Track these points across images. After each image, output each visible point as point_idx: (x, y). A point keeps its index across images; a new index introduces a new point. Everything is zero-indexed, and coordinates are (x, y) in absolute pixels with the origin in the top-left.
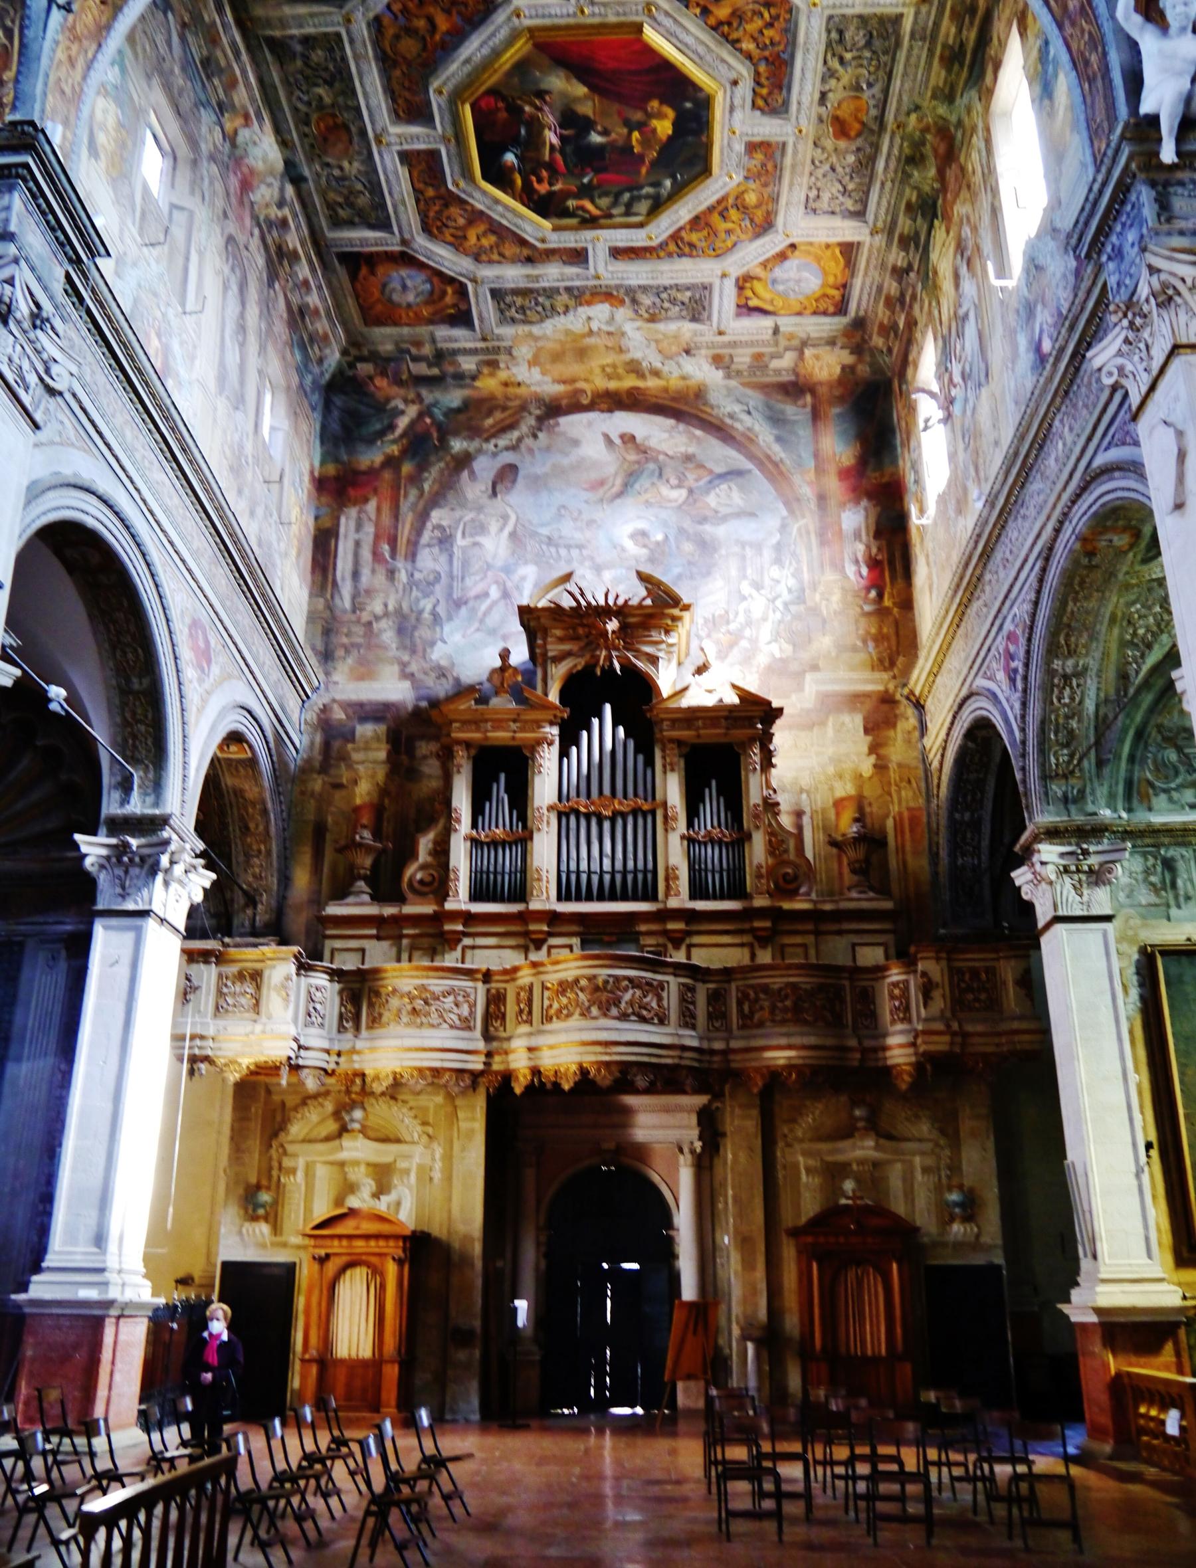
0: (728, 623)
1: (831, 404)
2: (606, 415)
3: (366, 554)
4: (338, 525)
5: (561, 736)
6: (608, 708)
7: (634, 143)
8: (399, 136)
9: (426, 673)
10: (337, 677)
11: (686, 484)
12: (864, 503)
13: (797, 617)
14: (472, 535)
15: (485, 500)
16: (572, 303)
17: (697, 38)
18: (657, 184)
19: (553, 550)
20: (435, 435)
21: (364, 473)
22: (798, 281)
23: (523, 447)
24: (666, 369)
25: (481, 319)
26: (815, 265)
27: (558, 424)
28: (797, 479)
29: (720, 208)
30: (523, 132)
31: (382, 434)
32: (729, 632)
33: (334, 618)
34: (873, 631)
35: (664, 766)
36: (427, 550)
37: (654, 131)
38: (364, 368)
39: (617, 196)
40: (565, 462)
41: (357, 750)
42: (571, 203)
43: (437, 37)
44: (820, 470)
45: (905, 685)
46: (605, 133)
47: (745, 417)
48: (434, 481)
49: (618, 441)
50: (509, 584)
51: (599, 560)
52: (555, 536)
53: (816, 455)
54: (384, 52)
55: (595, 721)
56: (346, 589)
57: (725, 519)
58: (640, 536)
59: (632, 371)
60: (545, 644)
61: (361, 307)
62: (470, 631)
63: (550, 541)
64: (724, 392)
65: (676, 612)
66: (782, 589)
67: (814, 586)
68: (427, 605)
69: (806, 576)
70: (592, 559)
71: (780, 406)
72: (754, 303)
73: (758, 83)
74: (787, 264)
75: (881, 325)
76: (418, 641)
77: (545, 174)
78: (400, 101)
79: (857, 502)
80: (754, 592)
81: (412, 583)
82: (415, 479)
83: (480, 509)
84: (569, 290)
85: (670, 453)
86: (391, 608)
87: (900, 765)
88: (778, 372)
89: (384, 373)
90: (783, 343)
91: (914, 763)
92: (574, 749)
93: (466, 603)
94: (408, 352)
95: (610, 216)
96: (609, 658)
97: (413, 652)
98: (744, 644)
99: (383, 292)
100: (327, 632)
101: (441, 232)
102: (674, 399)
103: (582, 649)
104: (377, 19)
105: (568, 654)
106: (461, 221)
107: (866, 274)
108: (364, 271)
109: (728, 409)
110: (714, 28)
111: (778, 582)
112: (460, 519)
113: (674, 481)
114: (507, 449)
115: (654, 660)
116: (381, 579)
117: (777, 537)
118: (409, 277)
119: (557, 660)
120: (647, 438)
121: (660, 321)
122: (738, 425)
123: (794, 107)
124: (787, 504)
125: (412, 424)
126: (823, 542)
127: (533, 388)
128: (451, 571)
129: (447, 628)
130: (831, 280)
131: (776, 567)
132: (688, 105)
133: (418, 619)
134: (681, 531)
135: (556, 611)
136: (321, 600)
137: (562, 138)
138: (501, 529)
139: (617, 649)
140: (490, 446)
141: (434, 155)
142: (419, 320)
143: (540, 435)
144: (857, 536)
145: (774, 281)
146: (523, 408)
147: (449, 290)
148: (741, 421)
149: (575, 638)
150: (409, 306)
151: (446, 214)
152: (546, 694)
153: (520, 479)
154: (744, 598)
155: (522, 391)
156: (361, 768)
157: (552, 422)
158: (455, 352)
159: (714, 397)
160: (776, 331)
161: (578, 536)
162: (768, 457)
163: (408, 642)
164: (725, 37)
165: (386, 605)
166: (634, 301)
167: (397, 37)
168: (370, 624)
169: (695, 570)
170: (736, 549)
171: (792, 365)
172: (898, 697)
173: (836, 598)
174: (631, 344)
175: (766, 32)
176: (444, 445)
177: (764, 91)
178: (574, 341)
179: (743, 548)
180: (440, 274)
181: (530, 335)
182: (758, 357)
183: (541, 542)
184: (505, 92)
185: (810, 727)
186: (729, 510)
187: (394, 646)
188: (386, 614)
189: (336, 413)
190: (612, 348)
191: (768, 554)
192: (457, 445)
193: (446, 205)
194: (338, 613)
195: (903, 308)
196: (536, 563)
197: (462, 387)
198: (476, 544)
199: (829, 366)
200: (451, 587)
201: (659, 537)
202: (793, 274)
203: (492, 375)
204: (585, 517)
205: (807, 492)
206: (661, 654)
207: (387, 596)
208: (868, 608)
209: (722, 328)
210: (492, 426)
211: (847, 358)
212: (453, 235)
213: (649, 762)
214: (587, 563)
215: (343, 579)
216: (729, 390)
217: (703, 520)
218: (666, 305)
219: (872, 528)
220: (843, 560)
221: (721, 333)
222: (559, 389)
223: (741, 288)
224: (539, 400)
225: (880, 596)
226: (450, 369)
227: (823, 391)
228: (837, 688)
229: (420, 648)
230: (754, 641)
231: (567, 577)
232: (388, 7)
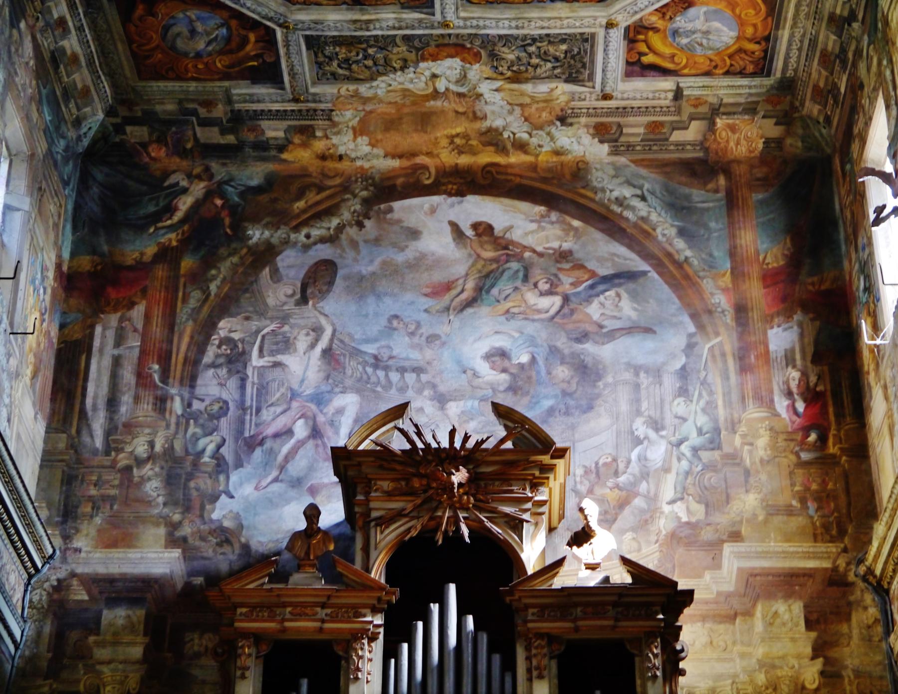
0: (616, 474)
1: (751, 188)
2: (454, 199)
3: (128, 376)
4: (91, 336)
5: (386, 625)
6: (452, 589)
9: (203, 539)
10: (78, 543)
11: (559, 289)
12: (798, 316)
13: (710, 467)
14: (272, 353)
15: (290, 306)
16: (412, 56)
19: (381, 373)
20: (227, 221)
21: (130, 268)
22: (707, 32)
23: (343, 237)
24: (534, 141)
25: (293, 75)
26: (728, 12)
27: (391, 210)
28: (707, 285)
31: (156, 217)
32: (617, 486)
33: (79, 461)
34: (814, 487)
35: (529, 671)
36: (211, 372)
38: (136, 133)
40: (400, 258)
41: (102, 644)
44: (737, 274)
45: (861, 561)
47: (636, 203)
48: (224, 280)
49: (469, 233)
50: (321, 419)
51: (442, 388)
52: (385, 354)
53: (733, 254)
55: (435, 608)
56: (98, 424)
57: (611, 335)
58: (498, 356)
59: (490, 144)
60: (368, 501)
61: (134, 55)
62: (264, 483)
63: (377, 362)
64: (612, 172)
65: (546, 459)
66: (689, 429)
67: (733, 426)
68: (208, 444)
69: (721, 413)
70: (434, 386)
71: (687, 190)
72: (649, 59)
75: (816, 87)
76: (195, 494)
79: (789, 317)
80: (652, 434)
81: (189, 416)
82: (199, 278)
83: (284, 319)
84: (407, 39)
85: (539, 249)
86: (158, 448)
87: (858, 673)
88: (681, 146)
89: (161, 141)
90: (687, 110)
91: (877, 671)
92: (405, 646)
93: (261, 443)
94: (194, 113)
96: (455, 521)
97: (187, 509)
98: (638, 502)
99: (164, 37)
100: (69, 480)
102: (544, 180)
103: (416, 508)
105: (398, 515)
107: (794, 25)
108: (140, 10)
109: (616, 194)
111: (685, 420)
112: (258, 332)
113: (544, 286)
114: (322, 240)
115: (516, 525)
116: (146, 409)
117: (683, 360)
118: (199, 18)
119: (384, 522)
120: (510, 228)
121: (527, 80)
122: (628, 214)
124: (694, 316)
125: (197, 206)
126: (744, 368)
127: (359, 163)
128: (243, 402)
129: (234, 477)
130: (750, 31)
131: (680, 400)
133: (196, 464)
134: (553, 351)
135: (384, 454)
136: (65, 435)
138: (312, 346)
139: (466, 509)
140: (302, 237)
142: (211, 73)
143: (367, 223)
144: (789, 359)
145: (675, 33)
146: (346, 188)
147: (252, 37)
148: (633, 209)
149: (410, 493)
150: (198, 55)
152: (368, 570)
153: (339, 281)
154: (638, 441)
155: (344, 165)
156: (105, 669)
157: (382, 206)
158: (258, 115)
159: (598, 178)
160: (678, 94)
161: (415, 355)
162: (669, 255)
163: (180, 495)
165: (152, 444)
166: (494, 56)
168: (128, 469)
169: (572, 403)
170: (628, 376)
171: (700, 138)
172: (851, 577)
173: (763, 441)
174: (488, 109)
176: (239, 235)
178: (414, 103)
179: (637, 374)
181: (356, 95)
182: (654, 127)
183: (365, 364)
185: (731, 618)
186: (617, 324)
187: (161, 500)
188: (151, 457)
189: (95, 190)
190: (464, 113)
191: (670, 382)
192: (256, 234)
194: (86, 455)
195: (844, 68)
196: (358, 391)
197: (264, 159)
198: (277, 365)
199: (747, 138)
200: (241, 422)
201: (525, 359)
202: (699, 24)
203: (305, 145)
204: (425, 330)
205: (721, 301)
206: (526, 516)
207: (155, 433)
208: (805, 456)
209: (608, 90)
210: (304, 211)
211: (773, 130)
213: (509, 666)
214: (426, 393)
215: (95, 408)
216: (618, 170)
217: (583, 337)
218: (535, 61)
219: (810, 350)
220: (771, 392)
221: (606, 97)
222: (396, 163)
224: (366, 177)
225: (823, 439)
226: (251, 137)
227: (740, 170)
228: (766, 564)
229: (197, 504)
230: (653, 499)
231: (400, 411)
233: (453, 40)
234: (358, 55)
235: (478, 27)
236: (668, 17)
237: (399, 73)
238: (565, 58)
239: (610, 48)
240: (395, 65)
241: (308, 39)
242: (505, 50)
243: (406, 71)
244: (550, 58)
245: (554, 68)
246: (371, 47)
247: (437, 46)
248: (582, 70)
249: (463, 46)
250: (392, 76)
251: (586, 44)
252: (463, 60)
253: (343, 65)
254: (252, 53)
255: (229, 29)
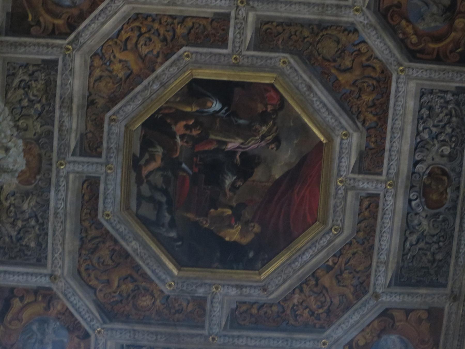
7: (219, 210)
8: (245, 19)
17: (306, 262)
18: (172, 225)
22: (41, 342)
29: (136, 276)
30: (242, 122)
37: (231, 227)
39: (165, 192)
42: (159, 151)
43: (333, 71)
46: (233, 187)
54: (326, 28)
72: (17, 304)
73: (262, 306)
74: (64, 332)
77: (195, 133)
78: (280, 29)
84: (50, 134)
95: (139, 181)
101: (132, 30)
104: (356, 31)
106: (144, 50)
110: (313, 275)
123: (236, 333)
132: (251, 254)
137: (233, 153)
141: (223, 43)
145: (43, 322)
151: (154, 38)
164: (306, 282)
166: (27, 194)
167: (338, 42)
175: (307, 311)
177: (254, 311)
180: (82, 17)
184: (281, 113)
193: (165, 40)
212: (127, 40)
218: (20, 224)
223: (36, 291)
232: (364, 42)
233: (44, 166)
234: (34, 95)
235: (58, 185)
236: (60, 316)
237: (12, 123)
238: (22, 245)
239: (30, 278)
240: (21, 122)
241: (55, 62)
242: (33, 203)
243: (15, 130)
244: (21, 234)
245: (11, 237)
246: (43, 106)
247: (40, 155)
248: (7, 256)
249: (39, 172)
250: (9, 118)
251: (35, 260)
252: (23, 172)
253: (23, 84)
254: (41, 19)
255: (69, 7)
